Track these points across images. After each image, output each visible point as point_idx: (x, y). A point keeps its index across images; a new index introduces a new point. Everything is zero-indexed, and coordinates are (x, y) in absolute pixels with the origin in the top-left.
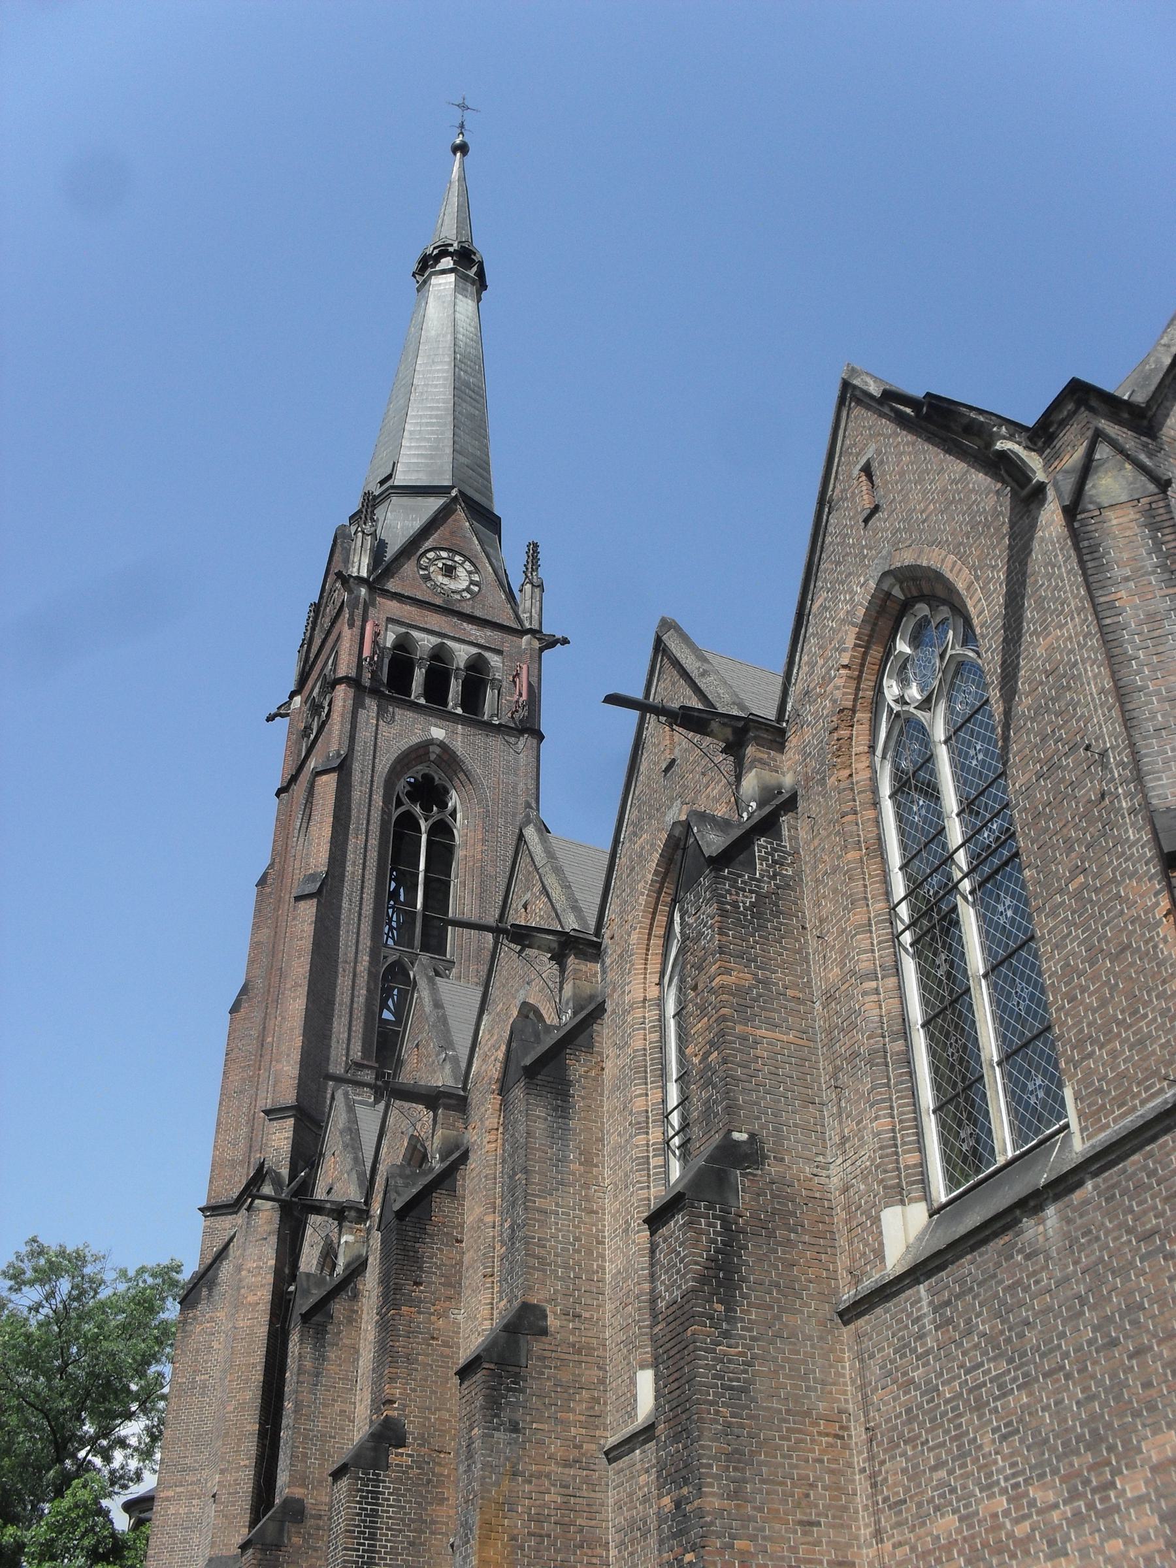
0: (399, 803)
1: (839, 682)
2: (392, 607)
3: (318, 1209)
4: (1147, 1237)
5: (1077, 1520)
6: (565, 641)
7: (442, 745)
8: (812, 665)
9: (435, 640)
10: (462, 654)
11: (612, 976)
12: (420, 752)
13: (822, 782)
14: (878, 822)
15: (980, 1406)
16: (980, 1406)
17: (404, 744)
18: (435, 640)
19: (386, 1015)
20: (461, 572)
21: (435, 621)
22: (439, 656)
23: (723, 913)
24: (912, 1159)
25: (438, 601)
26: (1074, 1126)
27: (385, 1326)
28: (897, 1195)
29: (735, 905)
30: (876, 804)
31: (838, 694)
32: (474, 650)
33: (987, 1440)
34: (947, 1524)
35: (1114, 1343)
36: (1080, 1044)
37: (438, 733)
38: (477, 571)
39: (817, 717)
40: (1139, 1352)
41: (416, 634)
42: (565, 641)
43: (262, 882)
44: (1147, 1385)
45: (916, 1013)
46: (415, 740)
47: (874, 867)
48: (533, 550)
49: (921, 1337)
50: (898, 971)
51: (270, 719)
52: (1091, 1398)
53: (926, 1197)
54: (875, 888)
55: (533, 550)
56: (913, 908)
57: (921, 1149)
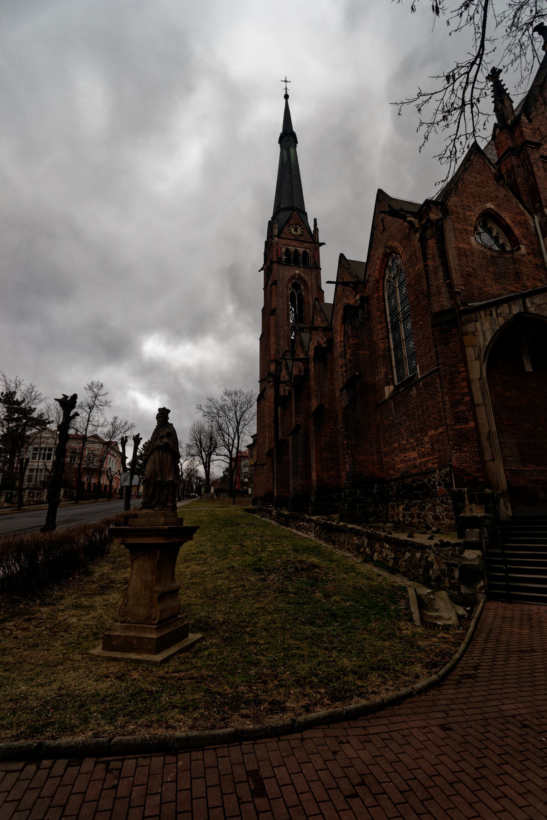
0: (290, 290)
1: (376, 273)
2: (283, 241)
3: (282, 382)
4: (431, 395)
6: (324, 244)
7: (298, 274)
8: (371, 268)
9: (294, 248)
10: (301, 250)
11: (334, 336)
12: (294, 277)
13: (373, 296)
14: (385, 305)
15: (401, 425)
16: (401, 425)
17: (288, 277)
18: (294, 248)
19: (292, 338)
20: (299, 230)
21: (295, 243)
22: (296, 251)
23: (352, 327)
24: (390, 377)
25: (294, 238)
26: (419, 373)
27: (296, 407)
28: (388, 384)
29: (355, 325)
30: (384, 301)
31: (376, 276)
32: (304, 249)
34: (396, 445)
35: (424, 414)
36: (420, 357)
37: (297, 272)
38: (302, 229)
39: (372, 281)
40: (429, 416)
41: (290, 247)
44: (430, 422)
45: (392, 346)
46: (292, 274)
47: (383, 316)
48: (315, 220)
49: (392, 411)
50: (388, 338)
51: (260, 271)
52: (420, 424)
53: (394, 384)
54: (383, 320)
55: (315, 220)
56: (391, 324)
57: (392, 374)
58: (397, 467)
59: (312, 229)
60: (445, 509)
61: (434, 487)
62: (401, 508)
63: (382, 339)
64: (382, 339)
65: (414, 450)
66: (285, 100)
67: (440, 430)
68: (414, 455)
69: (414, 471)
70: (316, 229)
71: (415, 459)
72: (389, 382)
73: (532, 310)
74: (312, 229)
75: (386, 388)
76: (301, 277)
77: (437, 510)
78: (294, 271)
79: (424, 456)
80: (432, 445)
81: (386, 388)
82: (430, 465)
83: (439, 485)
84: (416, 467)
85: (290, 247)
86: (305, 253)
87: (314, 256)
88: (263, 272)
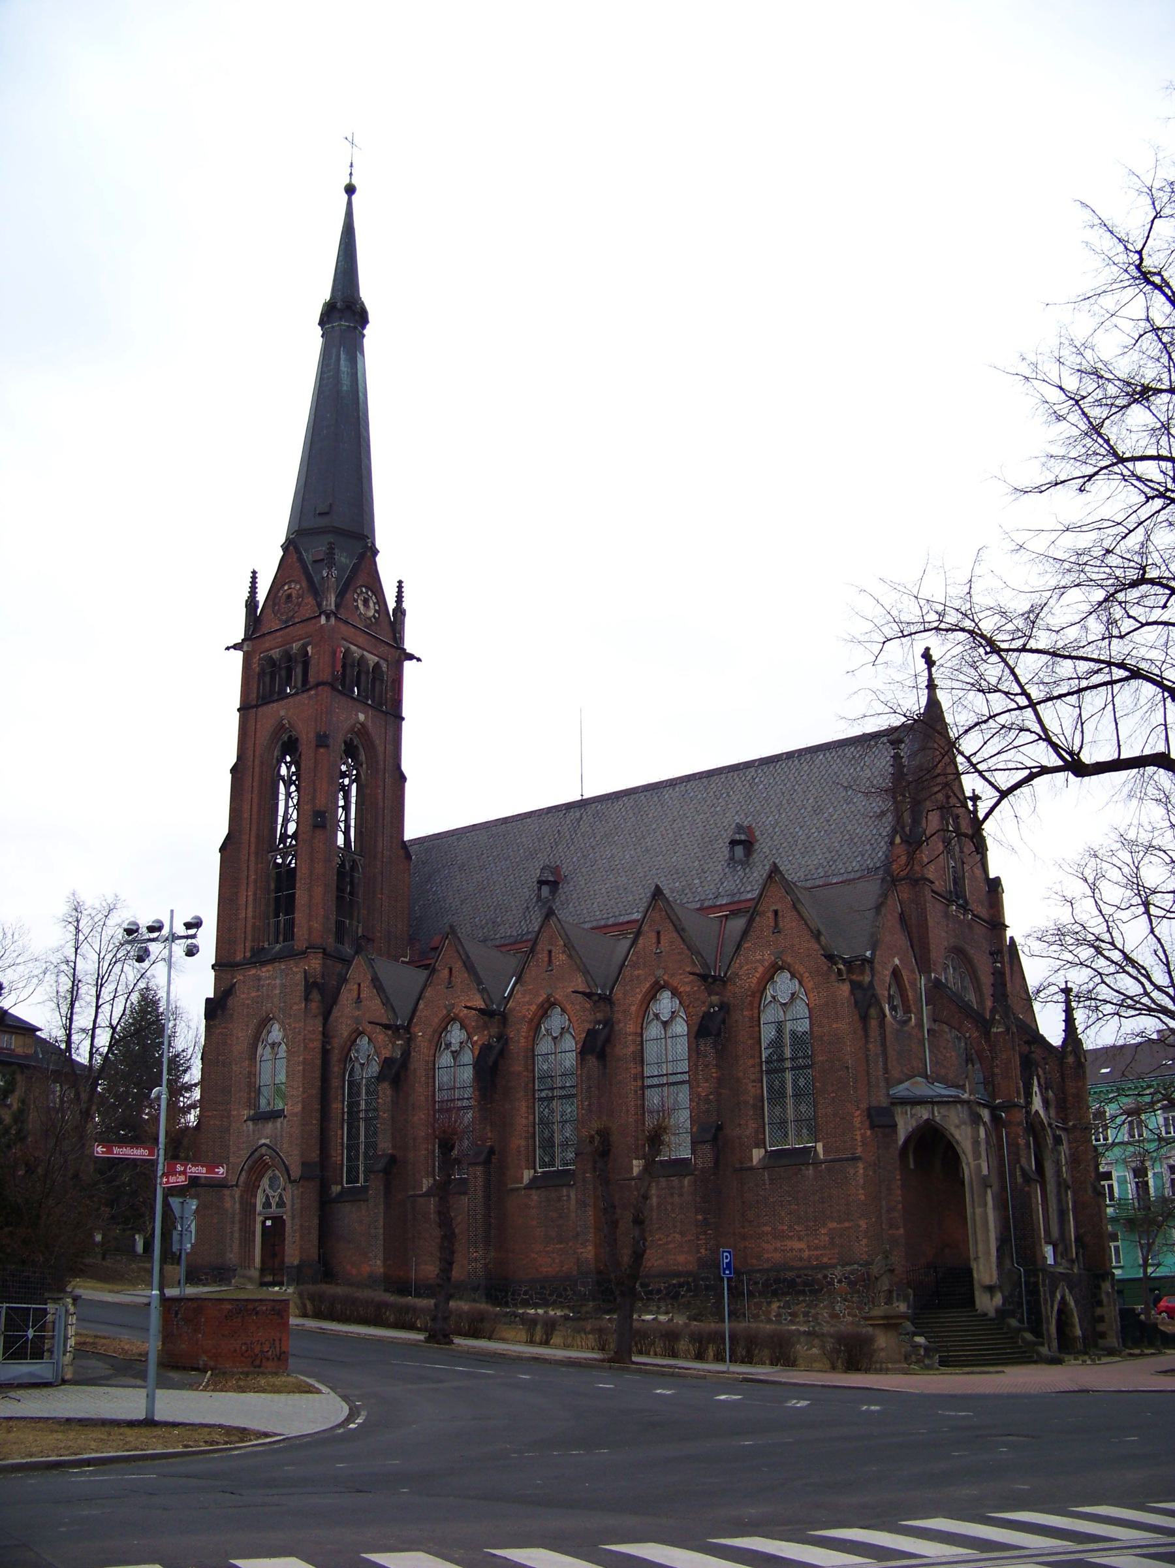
5: (807, 1235)
6: (419, 660)
16: (782, 1206)
18: (360, 651)
28: (757, 1146)
33: (783, 1214)
34: (768, 1229)
37: (362, 717)
42: (419, 660)
43: (234, 770)
47: (757, 1047)
48: (400, 582)
51: (228, 648)
53: (765, 1148)
54: (757, 1054)
57: (764, 1134)
58: (766, 1256)
59: (391, 605)
60: (848, 1307)
61: (831, 1283)
62: (775, 1306)
63: (754, 1081)
64: (754, 1081)
65: (800, 1239)
66: (346, 197)
67: (846, 1224)
68: (798, 1245)
69: (800, 1264)
70: (400, 611)
71: (800, 1250)
72: (761, 1144)
73: (938, 1119)
74: (391, 605)
75: (755, 1152)
76: (367, 733)
77: (837, 1308)
78: (357, 715)
79: (816, 1248)
80: (832, 1238)
81: (755, 1152)
82: (825, 1260)
83: (840, 1281)
84: (801, 1259)
85: (353, 648)
86: (377, 665)
87: (393, 681)
88: (239, 655)
